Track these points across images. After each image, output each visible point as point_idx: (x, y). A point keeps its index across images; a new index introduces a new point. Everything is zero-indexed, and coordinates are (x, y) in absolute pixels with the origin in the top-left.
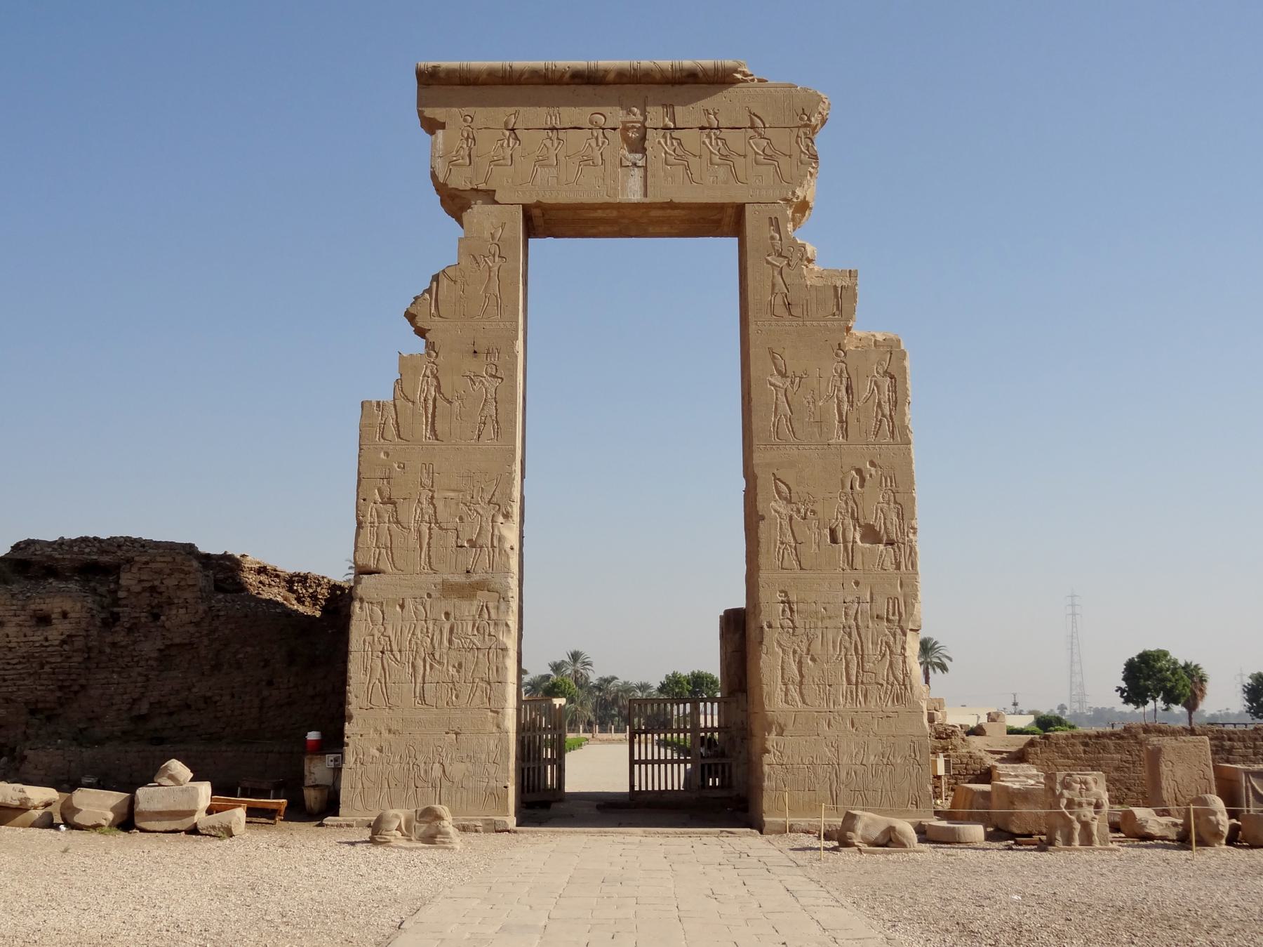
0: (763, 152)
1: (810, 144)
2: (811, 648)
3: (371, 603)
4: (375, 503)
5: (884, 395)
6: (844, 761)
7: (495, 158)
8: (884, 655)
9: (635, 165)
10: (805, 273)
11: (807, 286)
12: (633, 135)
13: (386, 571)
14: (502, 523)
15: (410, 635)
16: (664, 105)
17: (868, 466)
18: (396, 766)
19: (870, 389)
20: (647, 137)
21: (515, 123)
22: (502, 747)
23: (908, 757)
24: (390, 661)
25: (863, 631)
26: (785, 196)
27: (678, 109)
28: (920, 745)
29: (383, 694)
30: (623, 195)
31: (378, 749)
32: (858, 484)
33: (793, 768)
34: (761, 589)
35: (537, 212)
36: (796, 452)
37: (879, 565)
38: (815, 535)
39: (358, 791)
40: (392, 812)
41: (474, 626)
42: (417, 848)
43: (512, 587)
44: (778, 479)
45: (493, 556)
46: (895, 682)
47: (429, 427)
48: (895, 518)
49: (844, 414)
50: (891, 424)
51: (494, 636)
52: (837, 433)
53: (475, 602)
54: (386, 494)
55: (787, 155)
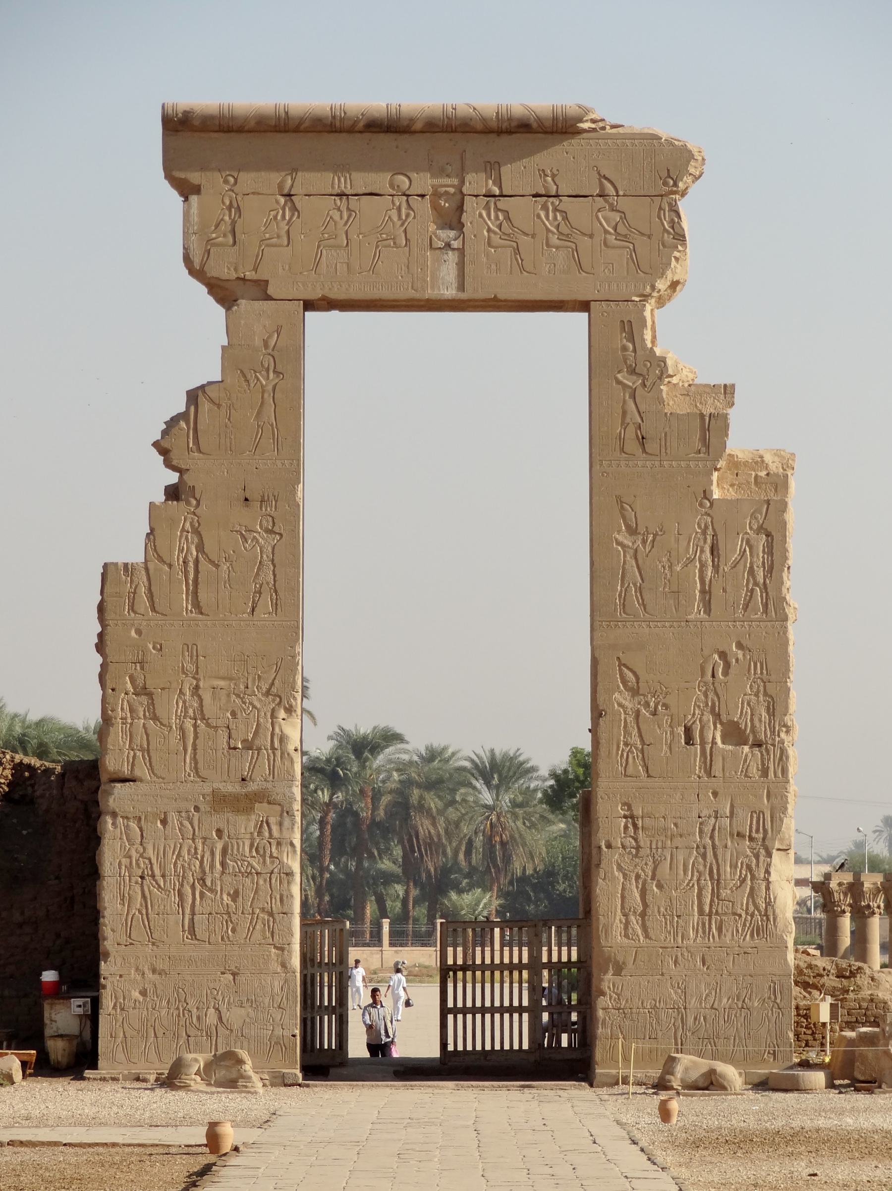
0: (615, 230)
1: (676, 220)
2: (657, 873)
3: (127, 818)
4: (126, 694)
5: (758, 557)
7: (267, 236)
9: (448, 245)
10: (664, 396)
11: (666, 414)
13: (143, 778)
14: (284, 719)
15: (175, 857)
18: (164, 1012)
19: (740, 550)
20: (465, 208)
21: (292, 186)
23: (766, 1000)
25: (720, 852)
26: (641, 291)
28: (782, 986)
29: (145, 927)
30: (433, 288)
31: (141, 993)
33: (631, 1013)
36: (647, 630)
37: (742, 771)
38: (666, 734)
39: (119, 1040)
40: (190, 1056)
41: (252, 846)
42: (218, 1092)
44: (625, 665)
45: (274, 760)
46: (756, 912)
47: (190, 598)
48: (764, 714)
50: (764, 594)
52: (698, 607)
53: (253, 817)
54: (140, 682)
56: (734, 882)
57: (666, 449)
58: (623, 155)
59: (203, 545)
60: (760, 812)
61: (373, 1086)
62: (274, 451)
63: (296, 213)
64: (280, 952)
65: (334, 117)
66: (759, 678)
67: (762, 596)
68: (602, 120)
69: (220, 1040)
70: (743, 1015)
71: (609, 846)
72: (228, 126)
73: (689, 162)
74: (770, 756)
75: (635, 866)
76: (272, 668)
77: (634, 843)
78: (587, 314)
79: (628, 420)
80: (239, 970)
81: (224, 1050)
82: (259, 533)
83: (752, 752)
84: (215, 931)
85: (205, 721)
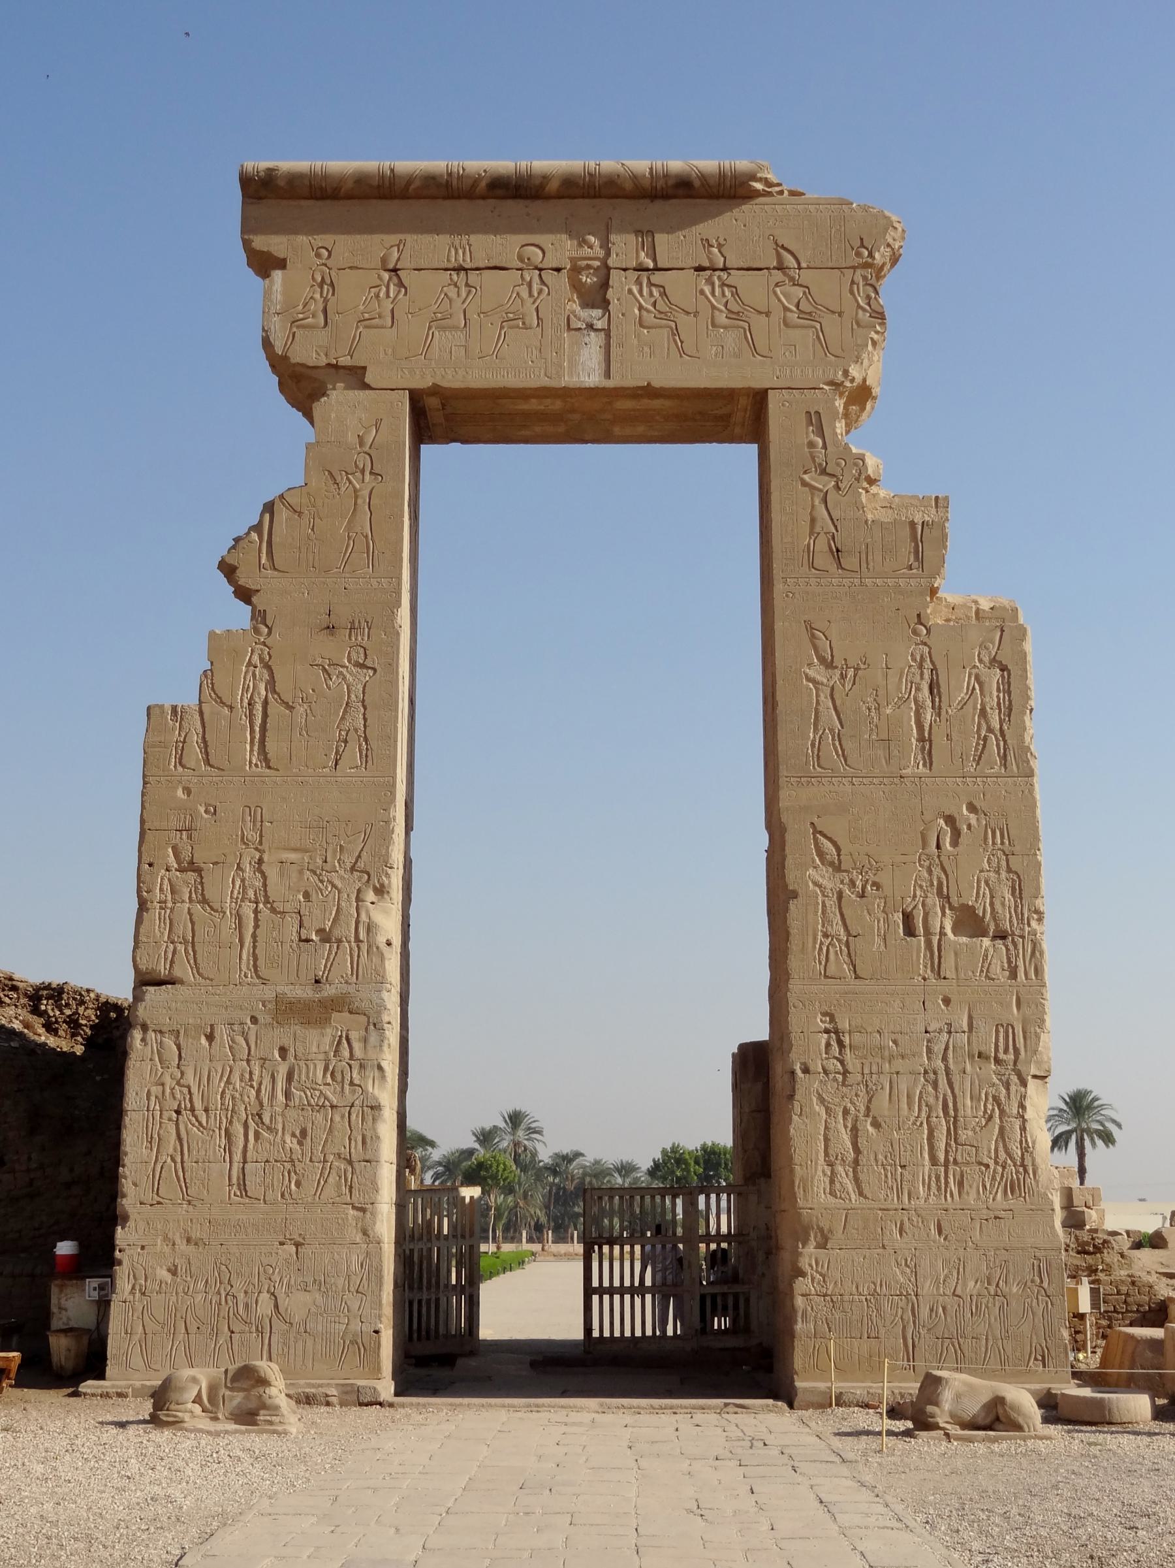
0: (798, 308)
1: (873, 295)
2: (871, 1107)
3: (161, 1032)
4: (167, 870)
6: (924, 1291)
7: (367, 316)
8: (991, 1117)
9: (590, 326)
10: (864, 500)
11: (866, 522)
12: (587, 279)
14: (373, 903)
15: (222, 1085)
16: (638, 232)
17: (965, 812)
18: (199, 1298)
19: (968, 688)
20: (611, 283)
21: (399, 259)
22: (371, 1266)
23: (1029, 1283)
24: (190, 1126)
25: (956, 1079)
26: (831, 377)
27: (660, 238)
28: (1049, 1264)
30: (571, 374)
31: (169, 1270)
32: (948, 840)
33: (842, 1301)
34: (792, 1010)
35: (433, 402)
36: (849, 788)
37: (982, 971)
38: (878, 922)
39: (136, 1338)
40: (187, 1372)
41: (326, 1069)
42: (227, 1432)
43: (388, 1007)
44: (821, 833)
45: (359, 956)
46: (1009, 1161)
47: (256, 748)
48: (1008, 896)
49: (927, 729)
50: (1002, 743)
51: (360, 1086)
52: (915, 758)
53: (329, 1031)
54: (186, 855)
55: (833, 312)
56: (977, 1120)
57: (867, 563)
58: (806, 222)
59: (275, 682)
60: (1008, 1025)
61: (483, 1406)
62: (369, 567)
63: (403, 290)
64: (360, 1214)
65: (450, 174)
66: (999, 849)
67: (998, 746)
68: (779, 185)
69: (274, 1339)
70: (997, 1305)
71: (806, 1070)
72: (321, 188)
73: (887, 230)
74: (1018, 950)
75: (843, 1097)
76: (360, 837)
77: (841, 1068)
78: (753, 449)
79: (818, 529)
80: (304, 1239)
81: (243, 1364)
82: (347, 667)
83: (994, 945)
84: (273, 1185)
85: (269, 906)
